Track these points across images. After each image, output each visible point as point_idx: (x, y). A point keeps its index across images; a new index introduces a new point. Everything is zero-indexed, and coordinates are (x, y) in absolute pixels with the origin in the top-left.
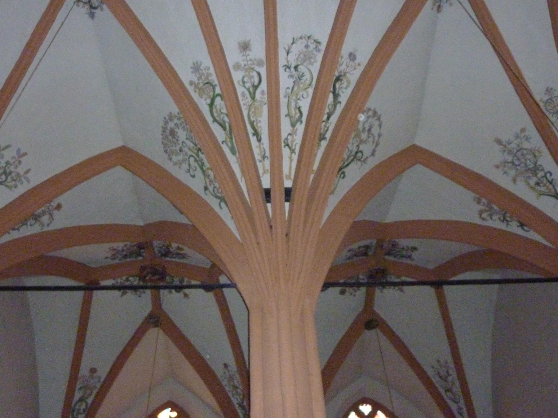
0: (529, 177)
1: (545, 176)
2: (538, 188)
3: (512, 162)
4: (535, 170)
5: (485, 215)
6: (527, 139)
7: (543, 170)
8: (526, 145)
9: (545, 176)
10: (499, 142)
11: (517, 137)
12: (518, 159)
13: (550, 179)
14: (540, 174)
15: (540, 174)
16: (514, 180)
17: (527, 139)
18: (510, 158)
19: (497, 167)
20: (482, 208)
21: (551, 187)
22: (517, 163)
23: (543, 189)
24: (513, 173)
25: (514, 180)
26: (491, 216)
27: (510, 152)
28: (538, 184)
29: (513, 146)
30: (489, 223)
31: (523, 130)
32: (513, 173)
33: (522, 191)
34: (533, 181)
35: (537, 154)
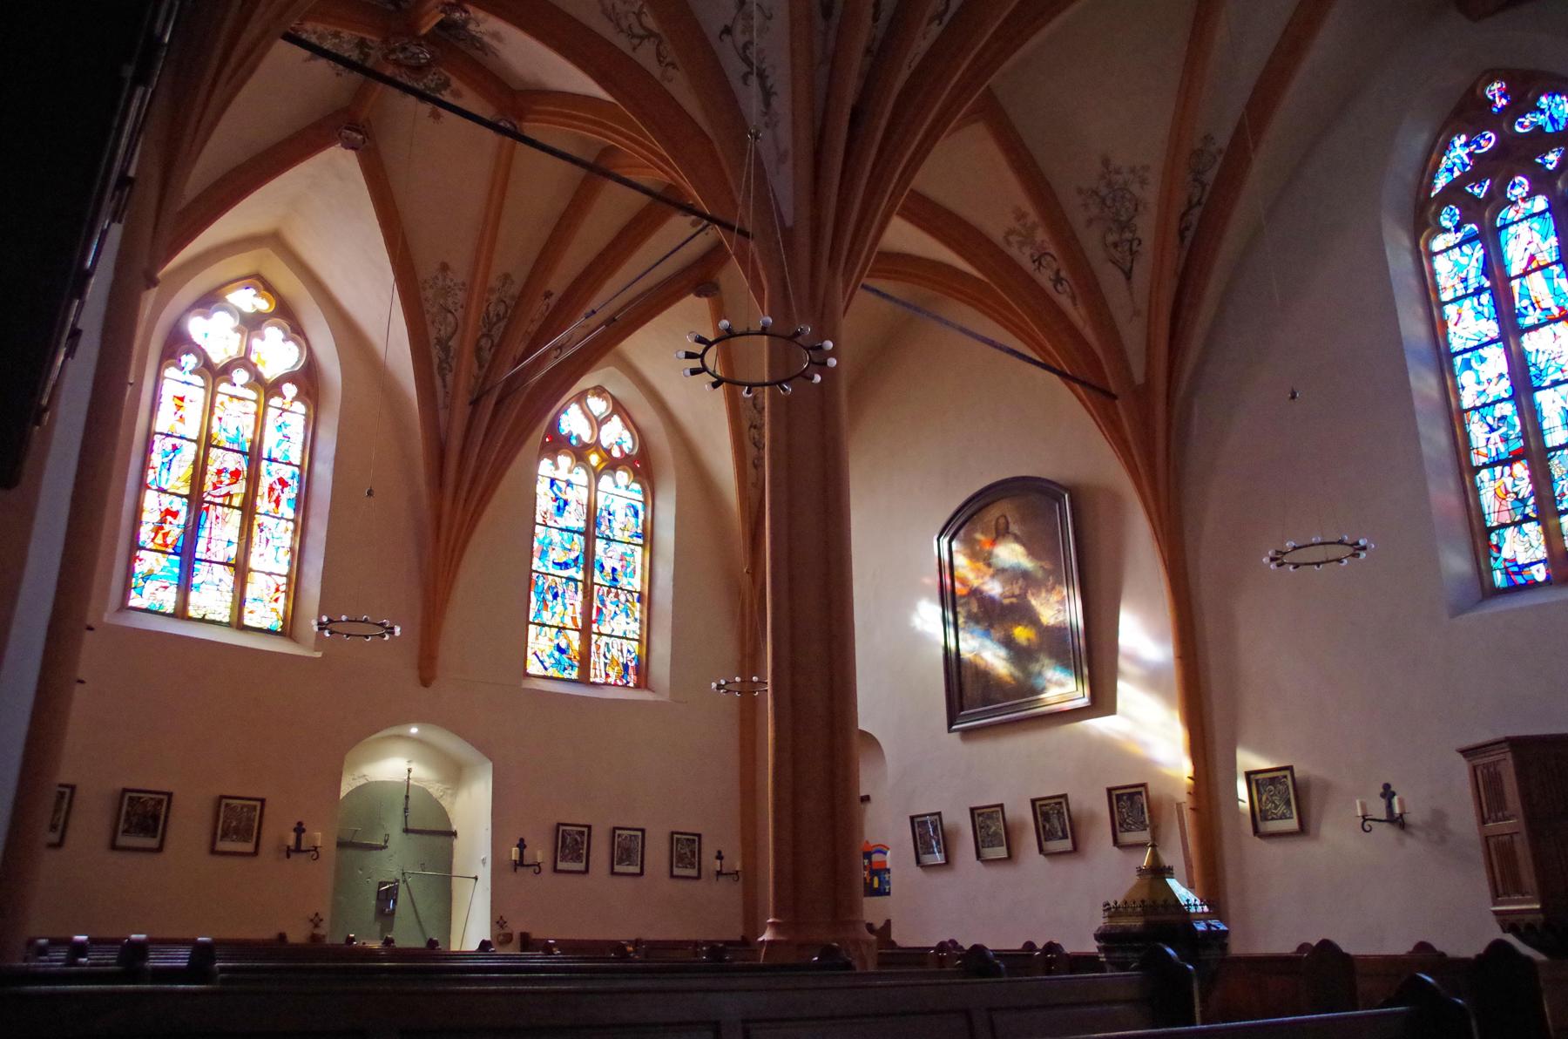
0: (1110, 229)
1: (1131, 242)
2: (1112, 250)
3: (1103, 200)
4: (1124, 226)
5: (1013, 239)
6: (1143, 182)
7: (1133, 232)
8: (1135, 188)
9: (1131, 242)
10: (1106, 162)
11: (1133, 171)
12: (1114, 200)
13: (1135, 247)
14: (1128, 235)
15: (1128, 235)
16: (1090, 222)
17: (1143, 182)
18: (1104, 191)
19: (1080, 191)
20: (1018, 227)
21: (1129, 258)
22: (1109, 202)
23: (1118, 256)
24: (1094, 211)
25: (1090, 222)
26: (1022, 244)
27: (1109, 184)
28: (1115, 245)
29: (1120, 179)
30: (1014, 251)
31: (1146, 168)
32: (1094, 211)
33: (1092, 242)
34: (1111, 238)
35: (1140, 208)
